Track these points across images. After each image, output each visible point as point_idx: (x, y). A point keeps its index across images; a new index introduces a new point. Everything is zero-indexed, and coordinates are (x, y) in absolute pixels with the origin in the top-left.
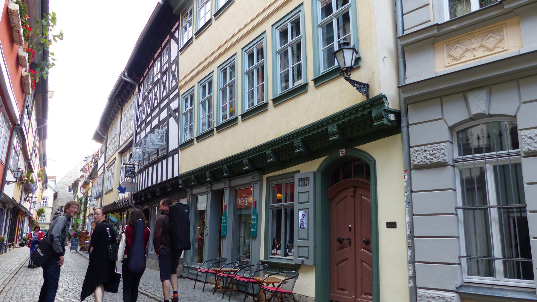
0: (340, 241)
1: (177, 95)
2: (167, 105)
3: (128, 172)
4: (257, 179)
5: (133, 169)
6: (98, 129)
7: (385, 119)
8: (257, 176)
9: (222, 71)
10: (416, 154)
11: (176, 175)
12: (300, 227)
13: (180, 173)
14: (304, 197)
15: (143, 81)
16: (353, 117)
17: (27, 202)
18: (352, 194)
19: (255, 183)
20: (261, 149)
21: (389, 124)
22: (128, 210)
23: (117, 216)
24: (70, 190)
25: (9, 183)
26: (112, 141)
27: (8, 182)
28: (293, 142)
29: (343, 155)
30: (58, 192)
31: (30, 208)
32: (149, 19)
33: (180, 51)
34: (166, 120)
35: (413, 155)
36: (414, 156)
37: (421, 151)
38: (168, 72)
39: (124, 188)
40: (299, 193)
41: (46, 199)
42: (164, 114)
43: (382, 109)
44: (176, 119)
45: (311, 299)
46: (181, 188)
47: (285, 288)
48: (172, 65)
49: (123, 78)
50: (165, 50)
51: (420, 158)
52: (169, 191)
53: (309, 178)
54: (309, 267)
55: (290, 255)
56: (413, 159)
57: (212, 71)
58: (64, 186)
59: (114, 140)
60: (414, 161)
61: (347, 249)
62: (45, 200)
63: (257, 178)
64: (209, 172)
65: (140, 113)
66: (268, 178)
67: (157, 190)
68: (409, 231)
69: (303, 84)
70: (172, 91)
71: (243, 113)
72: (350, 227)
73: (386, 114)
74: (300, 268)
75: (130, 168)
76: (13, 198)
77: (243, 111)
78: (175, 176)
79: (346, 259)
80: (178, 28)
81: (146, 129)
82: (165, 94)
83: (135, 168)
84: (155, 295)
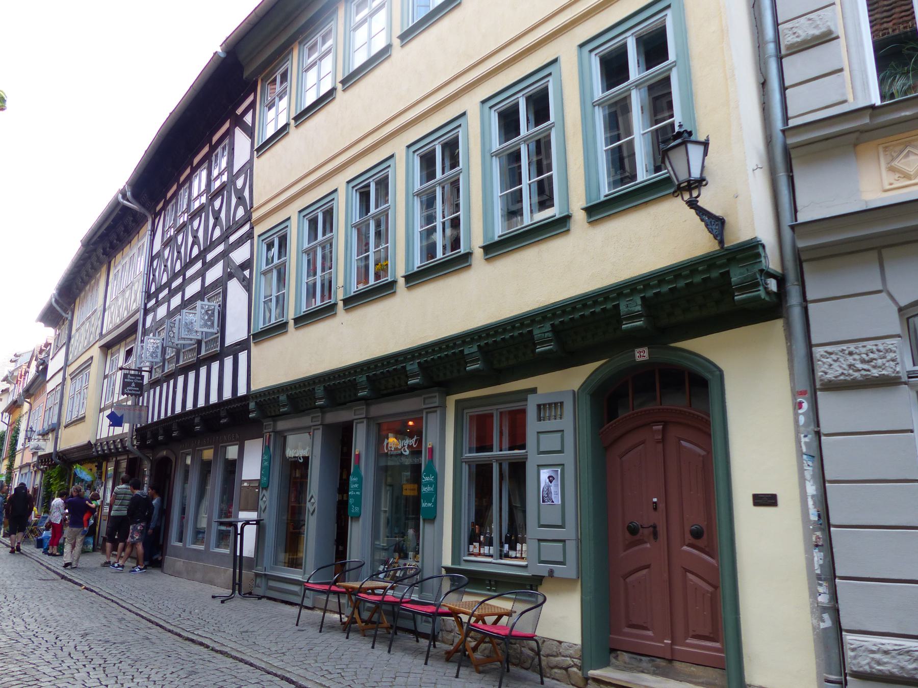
0: (633, 531)
1: (249, 236)
2: (223, 254)
3: (129, 384)
5: (139, 380)
6: (53, 300)
7: (761, 288)
8: (435, 397)
9: (356, 190)
10: (829, 360)
11: (242, 391)
12: (544, 501)
13: (253, 388)
14: (550, 442)
15: (164, 208)
16: (681, 284)
18: (660, 437)
21: (767, 299)
22: (118, 458)
23: (91, 470)
26: (83, 323)
28: (531, 332)
29: (643, 359)
32: (192, 86)
33: (258, 150)
34: (221, 284)
35: (822, 361)
36: (824, 363)
37: (841, 354)
38: (227, 192)
39: (119, 416)
40: (538, 433)
43: (756, 268)
44: (245, 283)
45: (571, 647)
46: (253, 418)
47: (523, 627)
48: (237, 178)
49: (122, 200)
50: (219, 150)
51: (838, 369)
52: (224, 423)
53: (562, 403)
54: (565, 583)
55: (514, 556)
56: (823, 369)
57: (333, 189)
60: (826, 373)
61: (648, 545)
63: (436, 402)
64: (322, 388)
65: (155, 271)
66: (457, 402)
68: (816, 513)
69: (558, 216)
70: (234, 228)
71: (409, 273)
72: (655, 503)
73: (763, 278)
74: (541, 584)
75: (133, 378)
77: (410, 268)
78: (239, 395)
79: (648, 567)
80: (252, 106)
82: (217, 233)
83: (143, 377)
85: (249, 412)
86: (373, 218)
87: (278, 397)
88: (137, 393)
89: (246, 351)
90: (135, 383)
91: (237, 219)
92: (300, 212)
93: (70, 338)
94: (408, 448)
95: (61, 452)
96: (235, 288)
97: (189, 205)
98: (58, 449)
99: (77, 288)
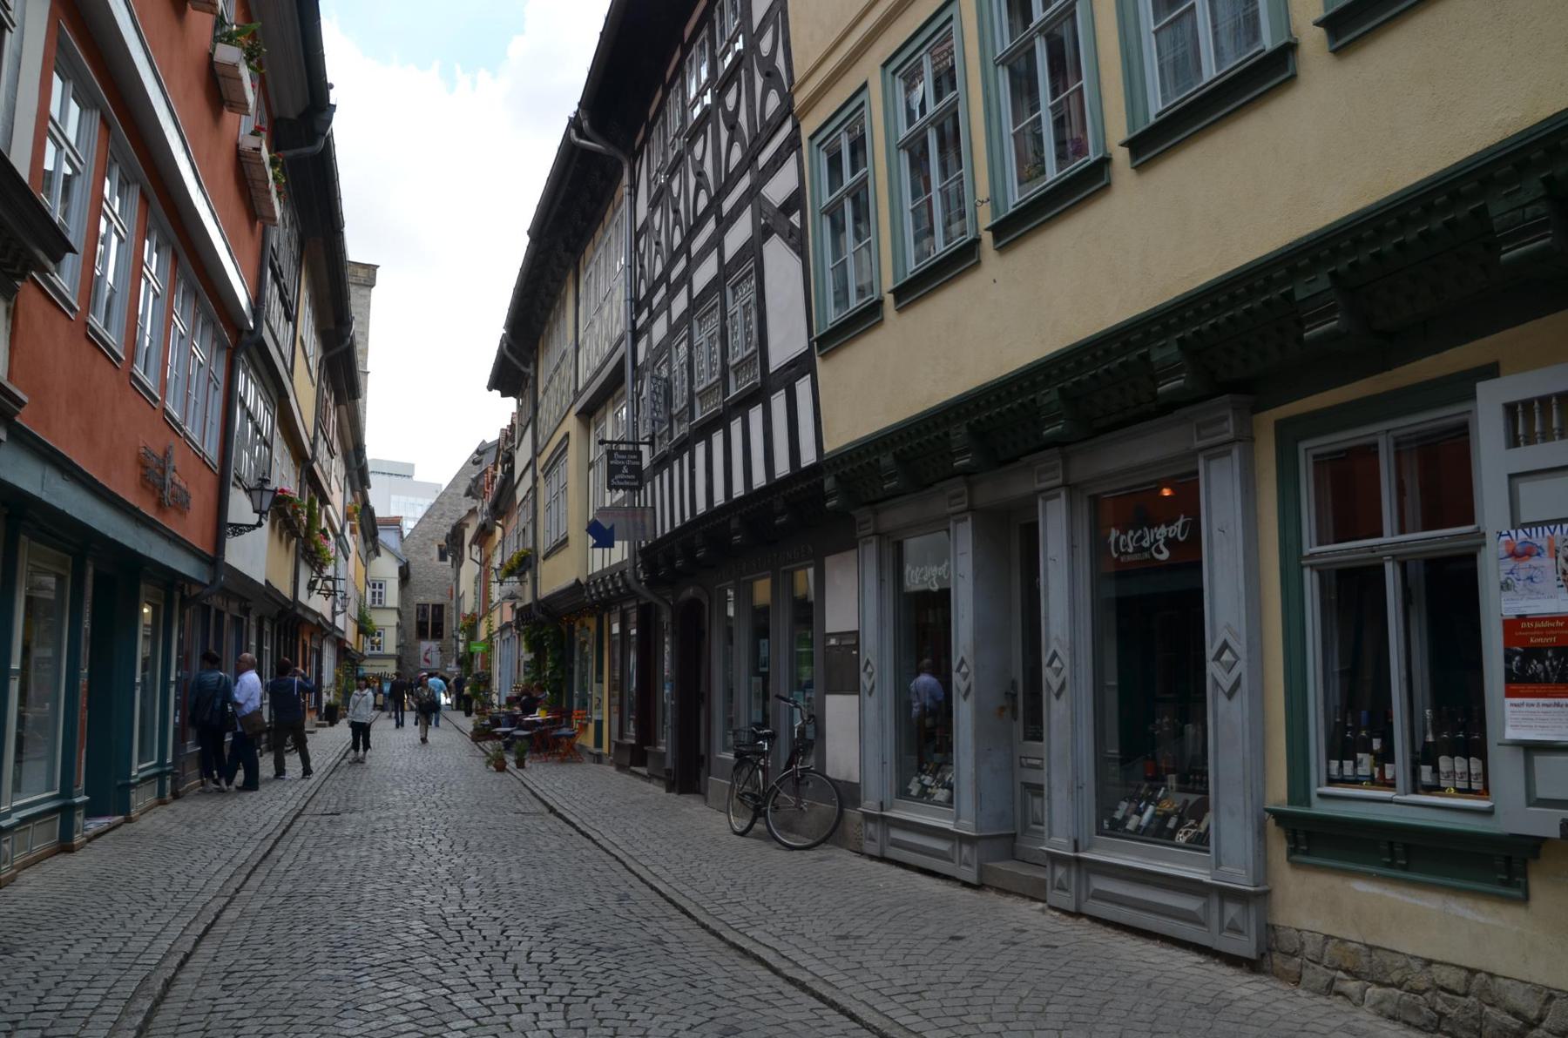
1: (793, 143)
2: (751, 193)
4: (1229, 436)
6: (505, 345)
8: (1225, 419)
13: (828, 448)
15: (646, 139)
19: (1217, 451)
20: (1262, 282)
22: (624, 607)
24: (443, 557)
25: (239, 529)
28: (1480, 214)
30: (412, 565)
31: (334, 613)
34: (752, 251)
38: (746, 70)
39: (607, 527)
40: (1511, 476)
41: (381, 586)
42: (739, 234)
49: (577, 140)
58: (425, 544)
59: (560, 374)
62: (377, 586)
63: (1229, 429)
64: (964, 430)
65: (642, 257)
67: (732, 526)
75: (623, 457)
76: (267, 582)
78: (803, 465)
81: (669, 308)
82: (737, 154)
83: (640, 454)
84: (796, 964)
85: (826, 498)
86: (1040, 31)
87: (877, 461)
88: (632, 484)
89: (809, 376)
91: (767, 118)
92: (885, 65)
93: (536, 409)
94: (1165, 544)
95: (543, 601)
96: (777, 253)
97: (684, 119)
98: (539, 596)
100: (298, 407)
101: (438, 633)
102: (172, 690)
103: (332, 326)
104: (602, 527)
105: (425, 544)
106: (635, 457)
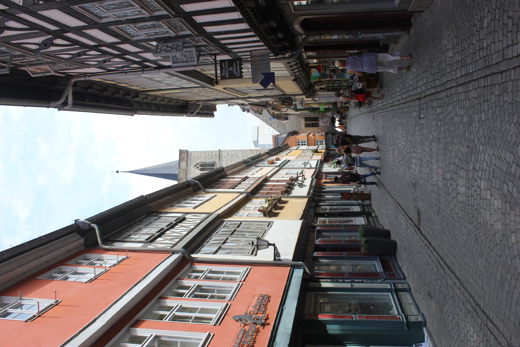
5: (225, 65)
17: (304, 182)
22: (305, 58)
25: (277, 254)
27: (276, 255)
31: (311, 168)
39: (263, 77)
41: (299, 142)
58: (282, 126)
75: (224, 71)
76: (301, 219)
83: (222, 61)
90: (229, 67)
95: (303, 92)
99: (178, 102)
100: (224, 206)
101: (316, 119)
102: (356, 285)
103: (191, 188)
104: (264, 78)
105: (282, 126)
106: (223, 64)
